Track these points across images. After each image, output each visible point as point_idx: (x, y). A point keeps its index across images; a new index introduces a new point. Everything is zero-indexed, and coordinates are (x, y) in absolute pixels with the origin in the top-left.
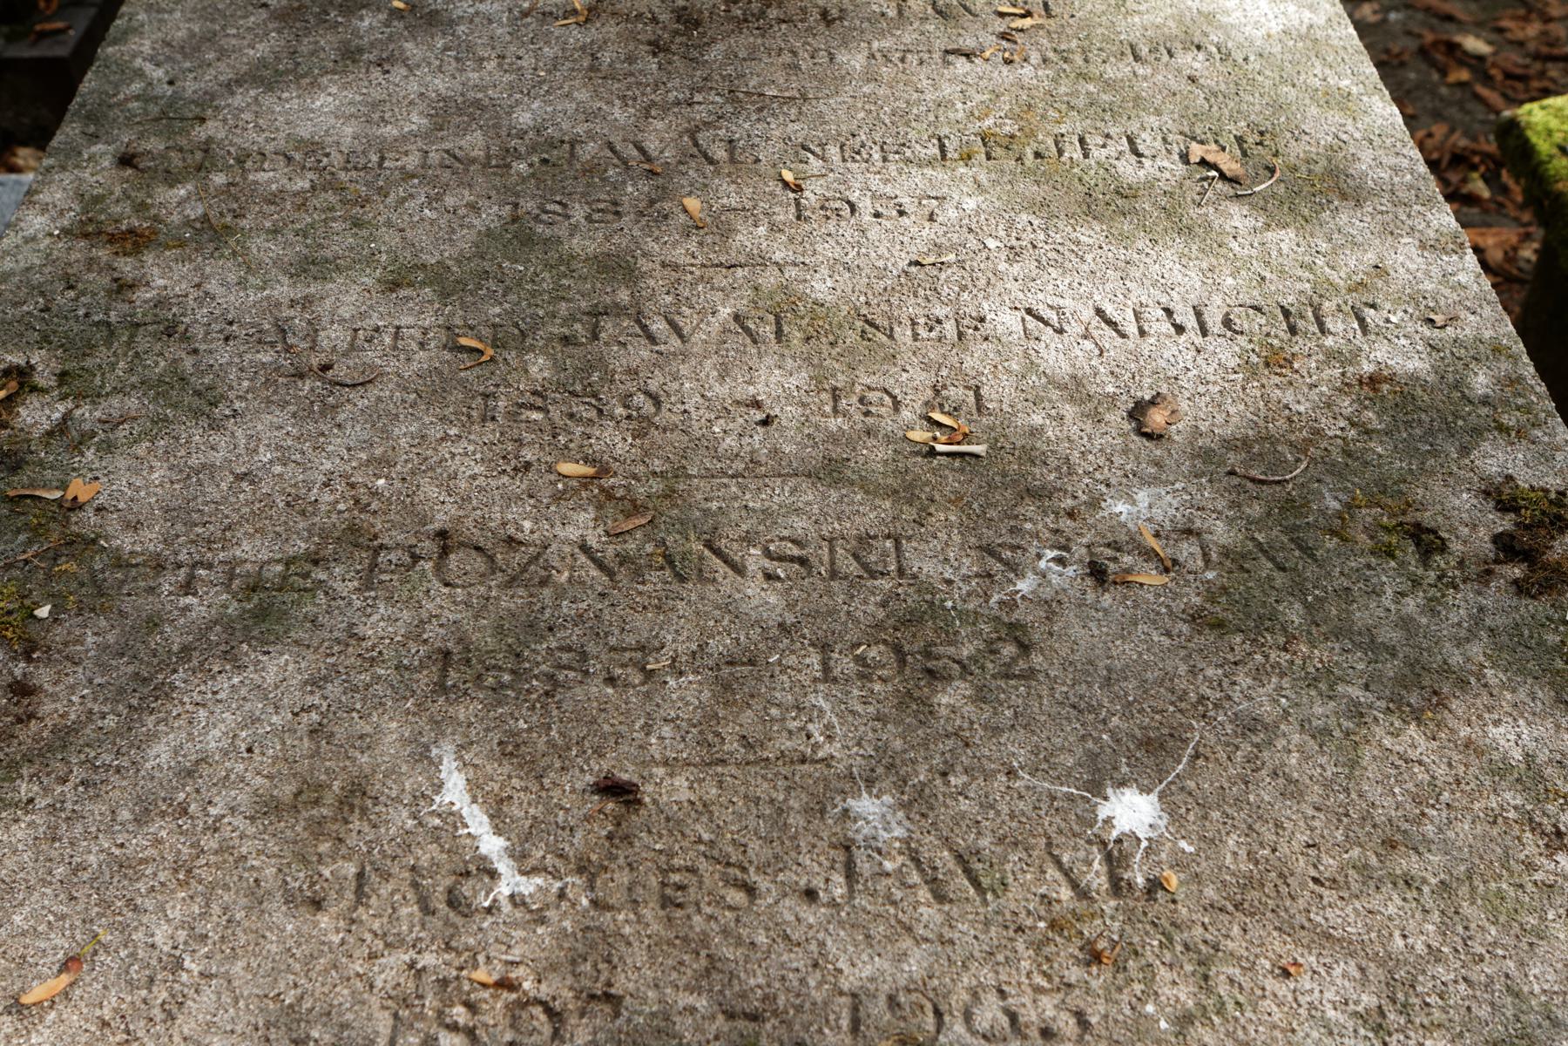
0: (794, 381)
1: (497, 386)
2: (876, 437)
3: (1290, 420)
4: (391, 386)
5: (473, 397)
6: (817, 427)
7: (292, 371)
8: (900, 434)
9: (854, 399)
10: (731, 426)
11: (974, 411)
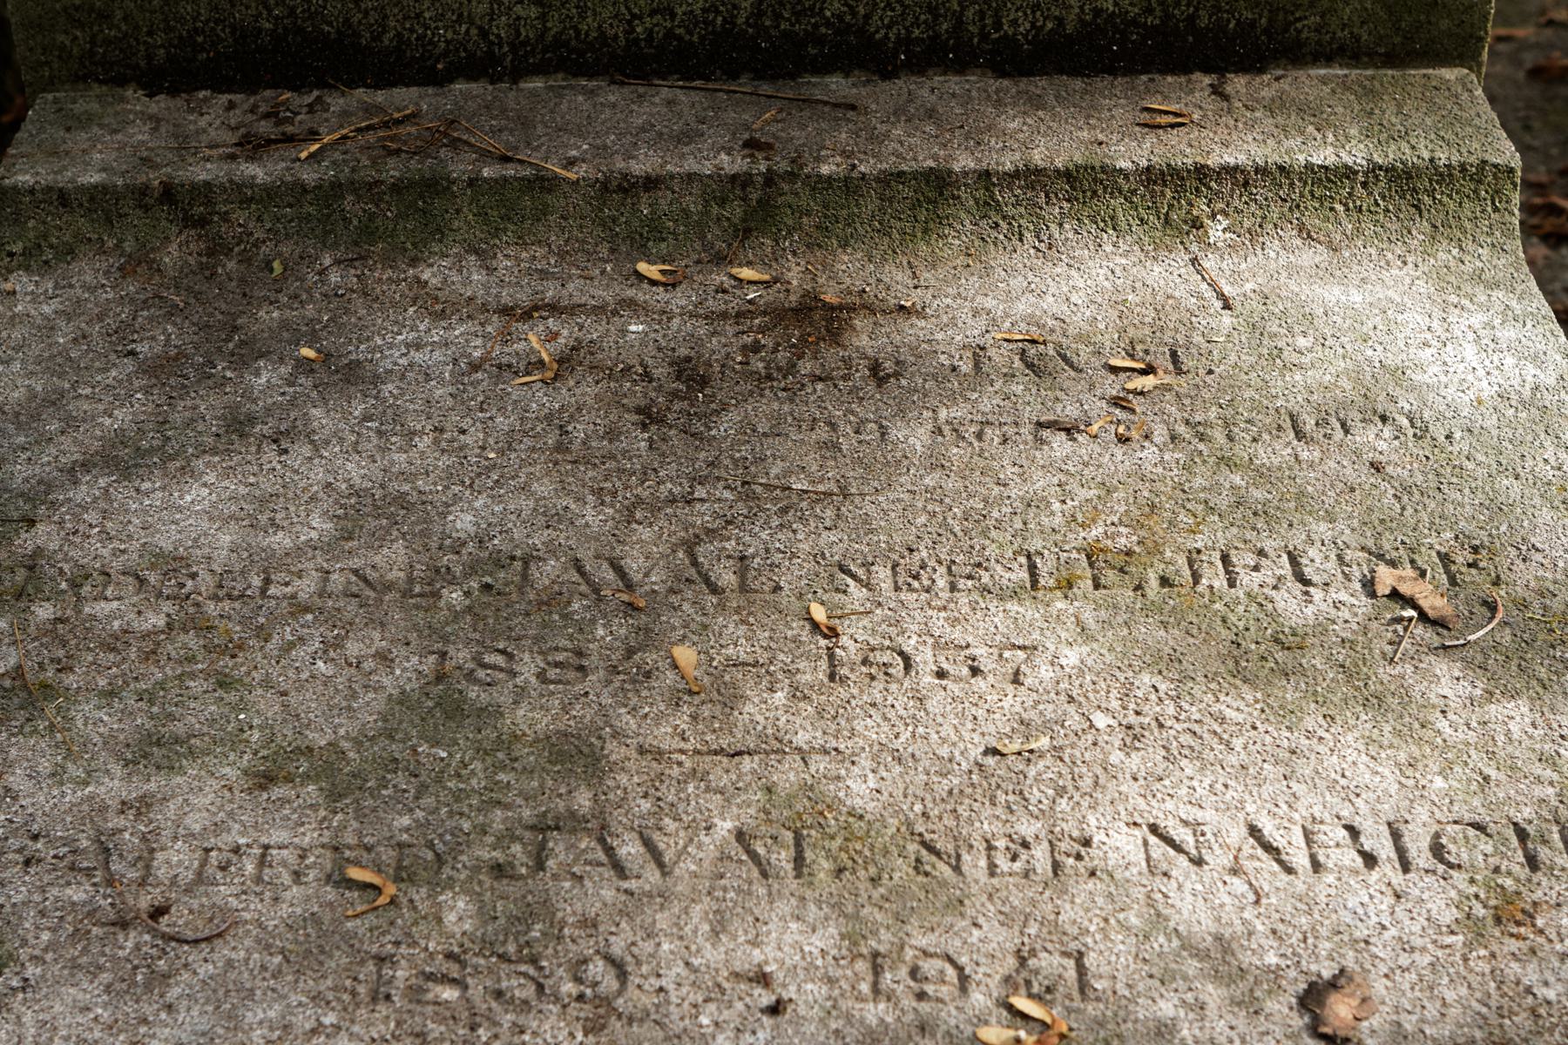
0: (815, 944)
1: (397, 944)
2: (933, 1035)
3: (1533, 1011)
4: (248, 942)
5: (362, 962)
6: (849, 1018)
7: (112, 916)
8: (968, 1030)
9: (903, 972)
10: (726, 1014)
11: (1076, 994)
